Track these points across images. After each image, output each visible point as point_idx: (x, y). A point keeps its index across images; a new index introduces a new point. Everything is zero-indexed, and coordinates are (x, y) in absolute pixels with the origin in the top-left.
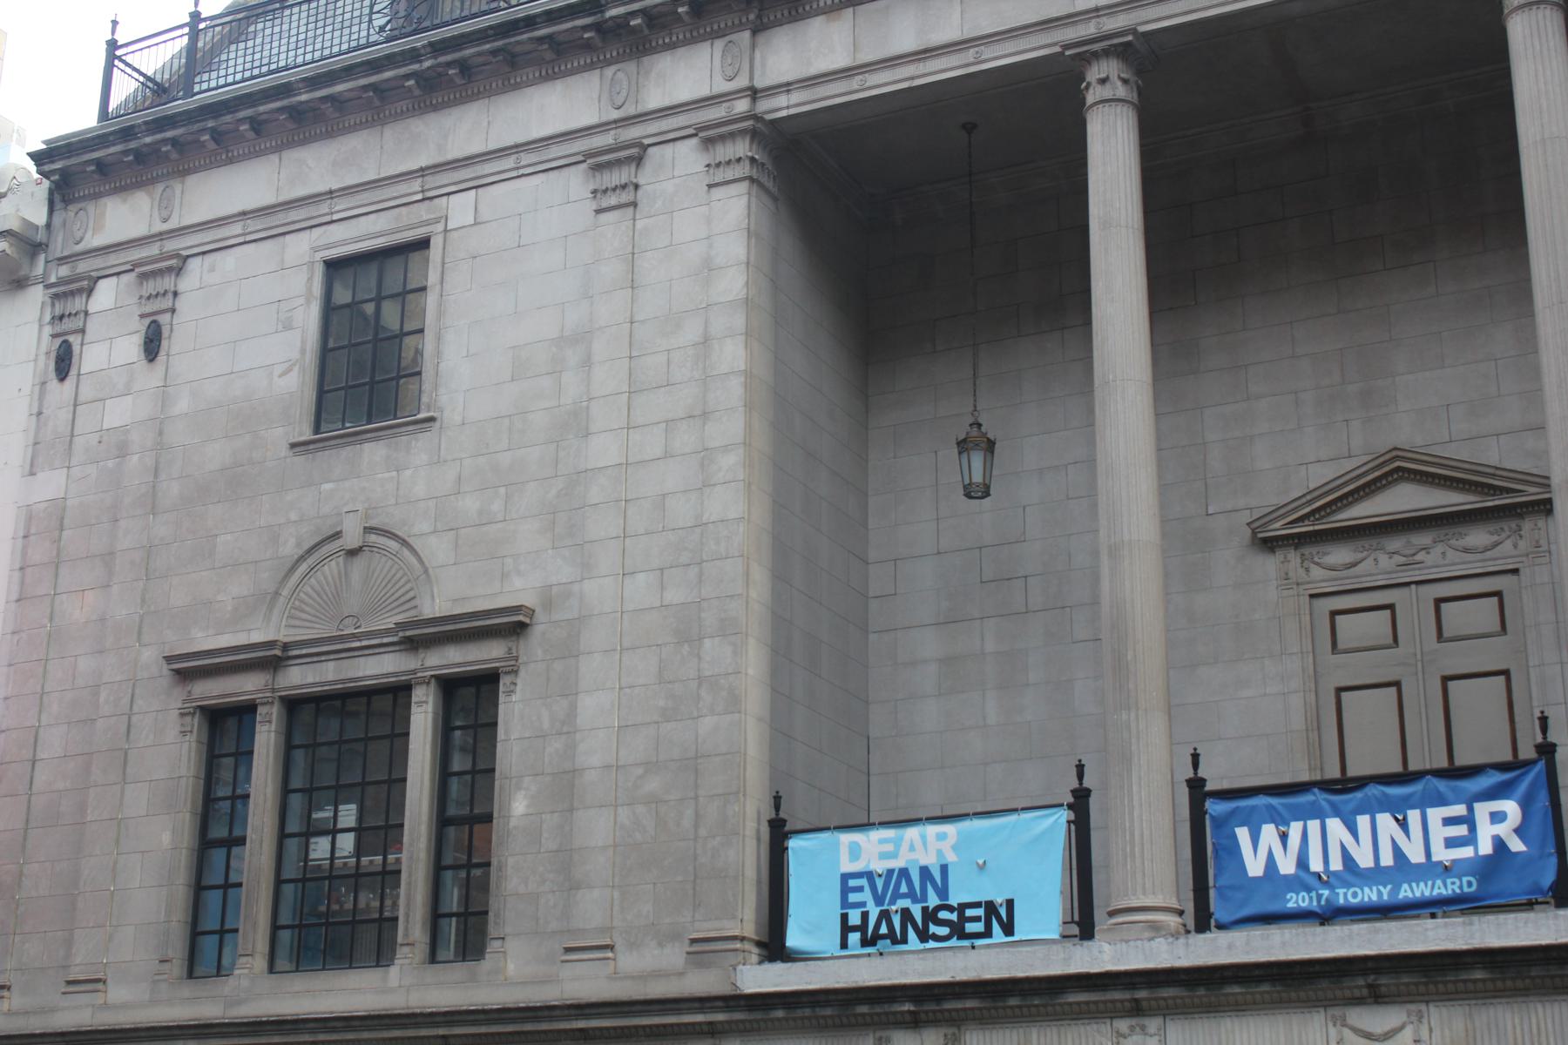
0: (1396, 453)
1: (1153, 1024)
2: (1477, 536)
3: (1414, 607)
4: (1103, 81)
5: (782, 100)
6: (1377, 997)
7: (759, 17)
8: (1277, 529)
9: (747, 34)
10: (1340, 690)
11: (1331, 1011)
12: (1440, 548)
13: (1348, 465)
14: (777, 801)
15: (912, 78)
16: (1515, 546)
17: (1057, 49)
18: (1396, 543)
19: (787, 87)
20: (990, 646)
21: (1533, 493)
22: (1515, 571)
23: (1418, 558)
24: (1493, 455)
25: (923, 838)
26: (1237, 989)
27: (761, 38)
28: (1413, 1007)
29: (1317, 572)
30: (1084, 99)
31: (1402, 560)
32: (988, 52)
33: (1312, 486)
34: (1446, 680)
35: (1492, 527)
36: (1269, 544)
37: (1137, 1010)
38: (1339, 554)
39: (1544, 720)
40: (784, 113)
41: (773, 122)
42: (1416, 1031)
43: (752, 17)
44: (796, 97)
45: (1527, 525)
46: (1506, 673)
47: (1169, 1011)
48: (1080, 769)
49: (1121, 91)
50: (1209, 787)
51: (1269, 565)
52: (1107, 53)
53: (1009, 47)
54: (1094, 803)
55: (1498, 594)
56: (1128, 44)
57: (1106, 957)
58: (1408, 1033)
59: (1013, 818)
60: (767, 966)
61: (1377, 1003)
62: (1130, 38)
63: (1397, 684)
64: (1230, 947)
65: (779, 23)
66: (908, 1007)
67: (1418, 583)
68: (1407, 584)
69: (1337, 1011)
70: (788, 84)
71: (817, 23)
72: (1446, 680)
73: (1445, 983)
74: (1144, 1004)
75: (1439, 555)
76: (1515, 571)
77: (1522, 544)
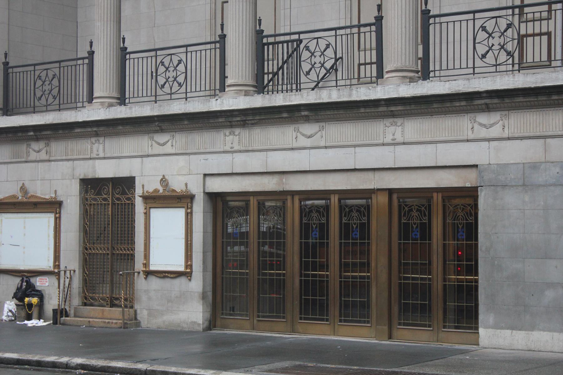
1: (101, 139)
6: (162, 131)
11: (150, 135)
14: (6, 55)
26: (121, 128)
28: (172, 134)
37: (97, 135)
42: (172, 142)
47: (105, 135)
57: (86, 115)
58: (170, 143)
60: (5, 117)
61: (162, 132)
64: (121, 112)
66: (32, 133)
69: (151, 135)
73: (321, 115)
74: (99, 132)
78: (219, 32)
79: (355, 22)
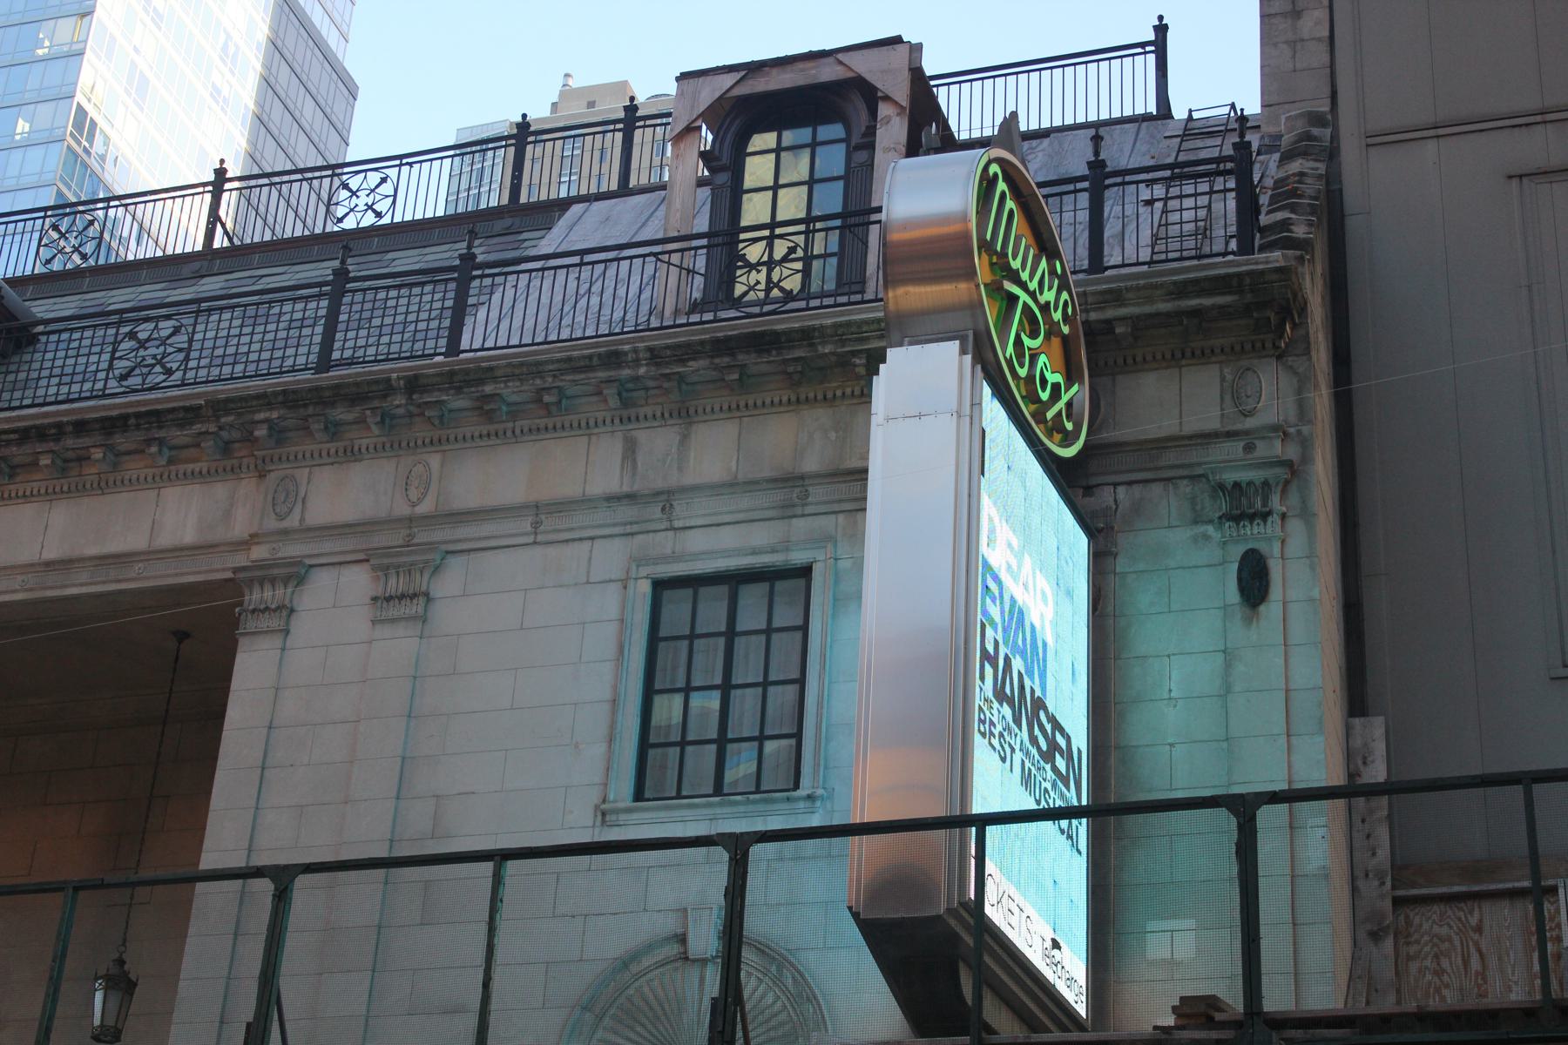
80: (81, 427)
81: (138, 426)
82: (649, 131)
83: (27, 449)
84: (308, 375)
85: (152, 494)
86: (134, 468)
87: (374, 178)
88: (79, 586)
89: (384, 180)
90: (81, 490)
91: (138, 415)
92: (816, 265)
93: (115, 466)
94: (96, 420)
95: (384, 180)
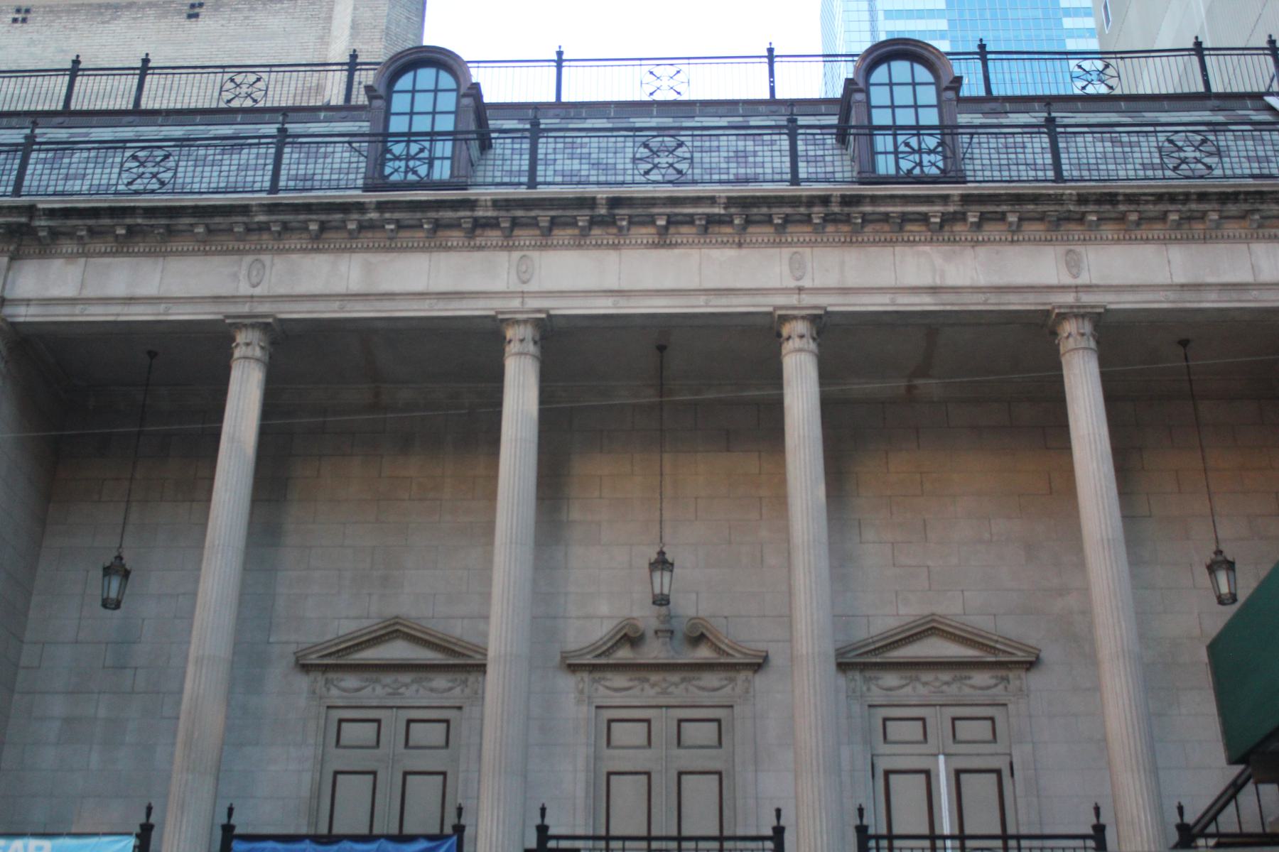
0: (396, 620)
2: (440, 681)
3: (393, 723)
4: (248, 344)
5: (22, 310)
7: (17, 250)
8: (313, 659)
9: (5, 260)
10: (336, 773)
12: (414, 687)
13: (366, 623)
15: (118, 315)
16: (463, 691)
17: (220, 317)
18: (388, 679)
19: (28, 302)
20: (102, 713)
21: (477, 659)
22: (460, 708)
23: (401, 690)
24: (458, 630)
25: (26, 848)
27: (17, 264)
29: (334, 692)
30: (232, 355)
31: (390, 691)
32: (174, 309)
33: (341, 633)
34: (406, 774)
35: (451, 676)
36: (306, 668)
38: (351, 681)
39: (460, 810)
40: (21, 319)
41: (13, 324)
43: (12, 248)
44: (33, 310)
45: (472, 678)
46: (444, 774)
48: (149, 810)
49: (258, 353)
50: (237, 831)
51: (303, 682)
52: (253, 326)
53: (189, 308)
54: (154, 834)
55: (447, 721)
56: (268, 324)
59: (94, 840)
62: (270, 320)
63: (374, 773)
65: (28, 256)
67: (398, 708)
68: (391, 707)
70: (29, 300)
71: (58, 263)
72: (406, 774)
75: (415, 692)
76: (460, 708)
77: (467, 691)
78: (451, 820)
79: (603, 832)
80: (1203, 197)
81: (1246, 201)
82: (363, 73)
83: (1161, 207)
84: (264, 195)
85: (1244, 247)
86: (1231, 228)
87: (252, 78)
88: (1210, 301)
89: (259, 80)
90: (1190, 239)
91: (1247, 193)
92: (437, 163)
93: (1218, 226)
94: (1216, 193)
95: (259, 80)
